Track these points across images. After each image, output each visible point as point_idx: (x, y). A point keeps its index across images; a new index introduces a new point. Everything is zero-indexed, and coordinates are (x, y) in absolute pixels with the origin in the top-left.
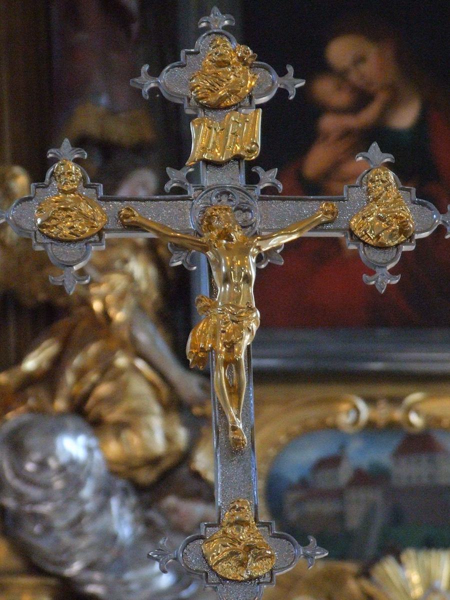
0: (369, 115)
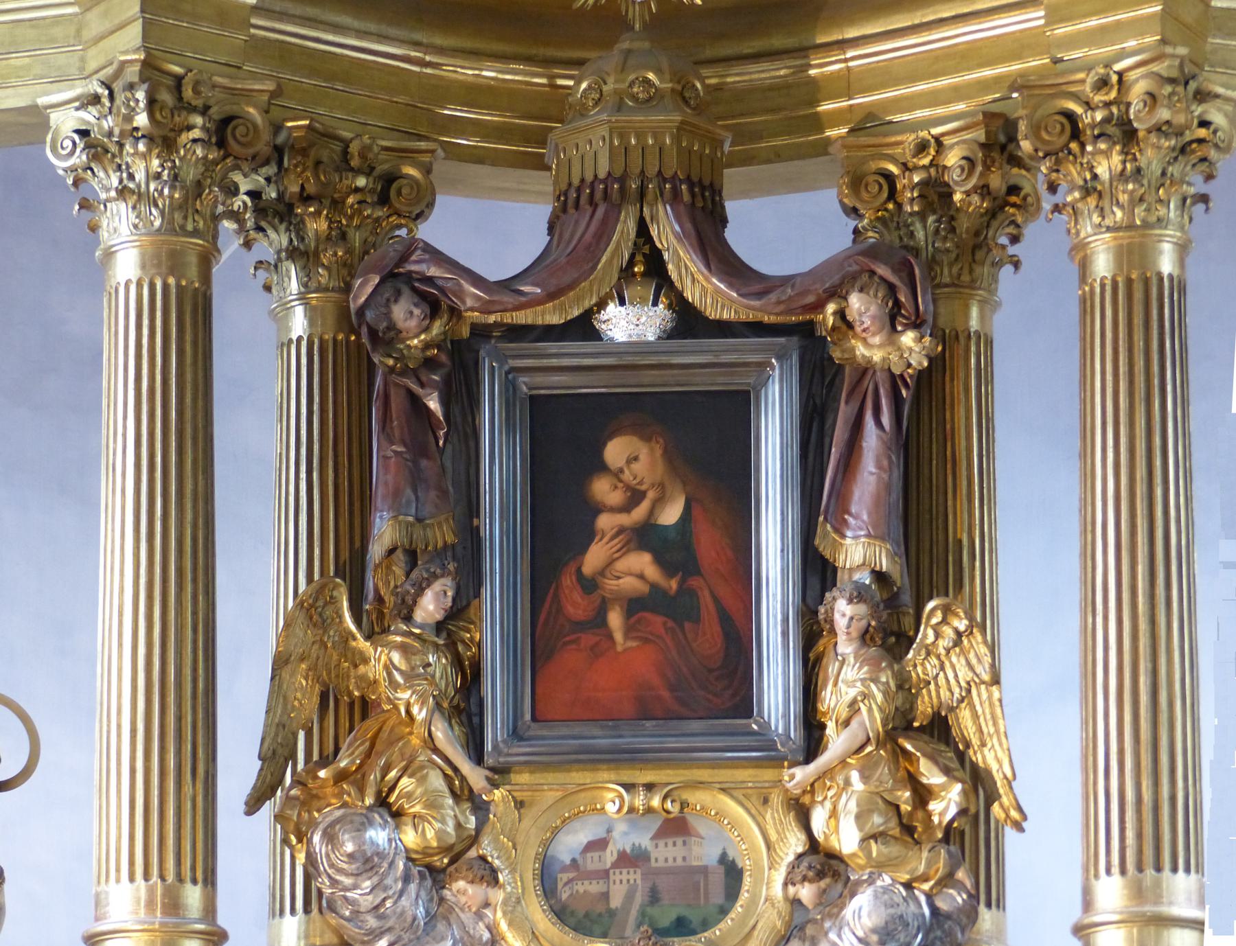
0: (640, 513)
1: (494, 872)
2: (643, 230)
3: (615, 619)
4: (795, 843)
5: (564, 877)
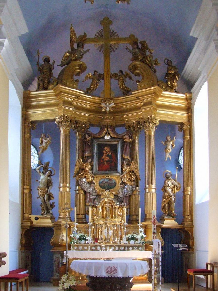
0: (107, 154)
1: (95, 183)
2: (107, 130)
3: (105, 162)
4: (121, 181)
5: (101, 184)
